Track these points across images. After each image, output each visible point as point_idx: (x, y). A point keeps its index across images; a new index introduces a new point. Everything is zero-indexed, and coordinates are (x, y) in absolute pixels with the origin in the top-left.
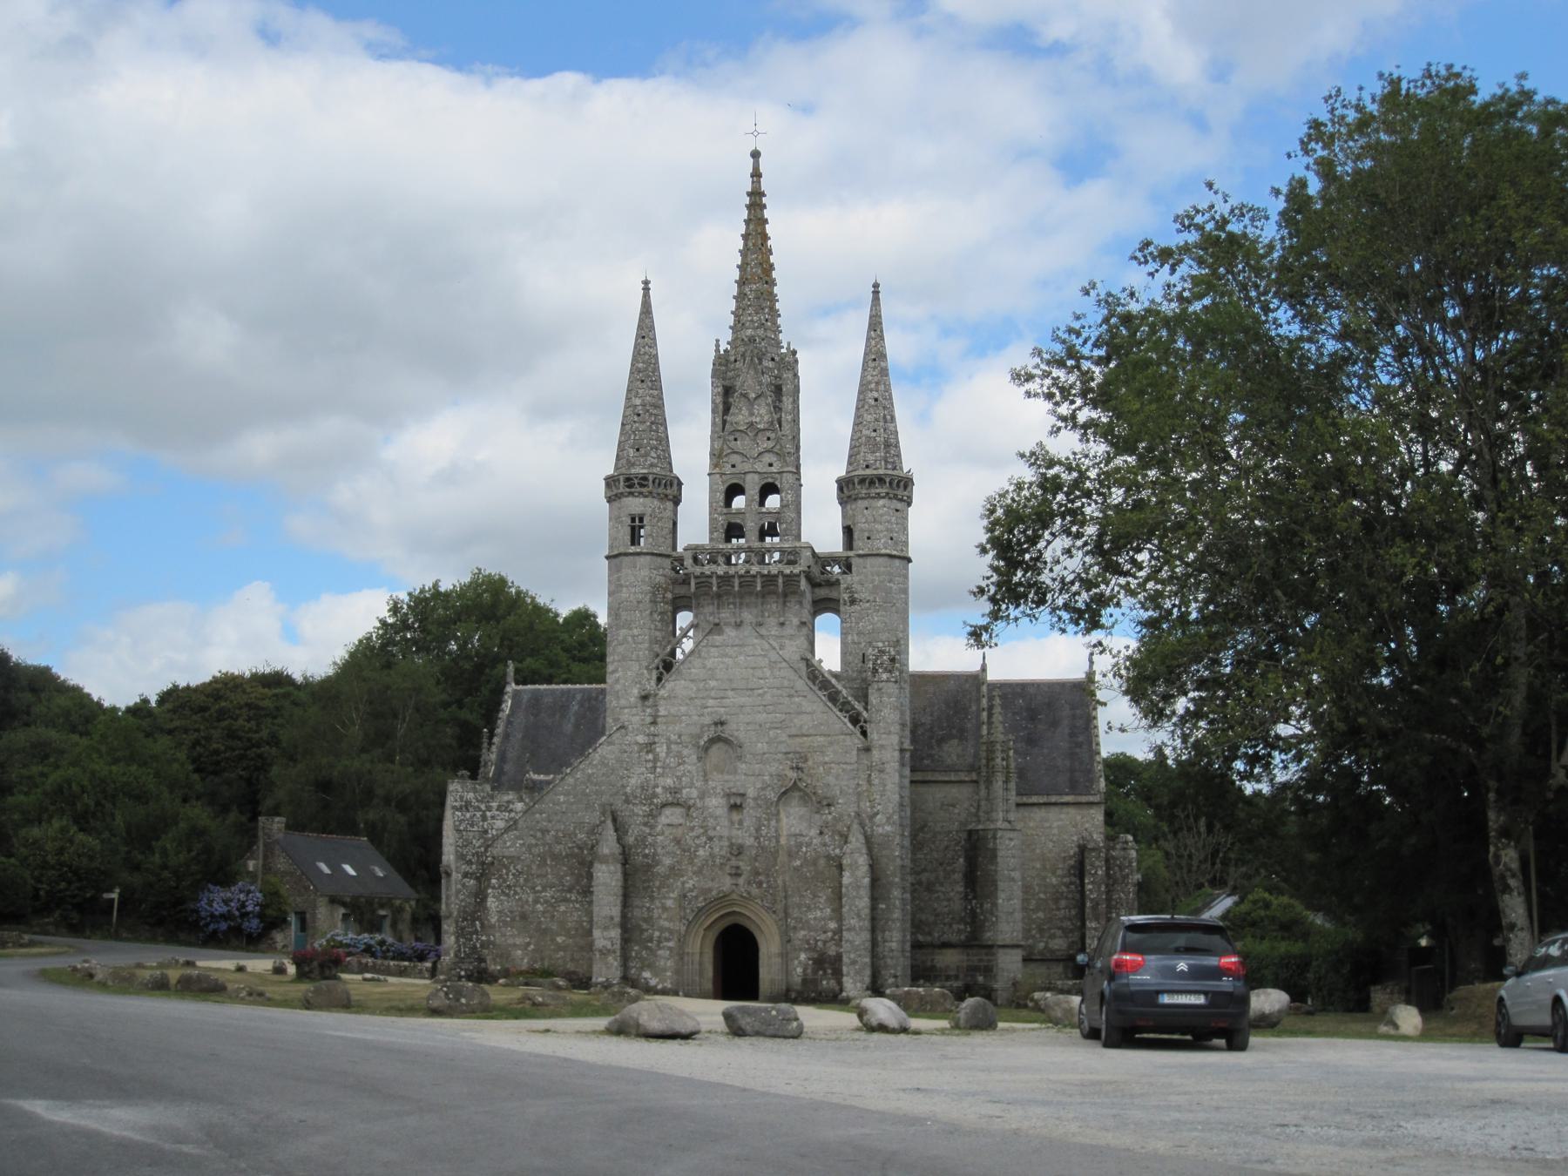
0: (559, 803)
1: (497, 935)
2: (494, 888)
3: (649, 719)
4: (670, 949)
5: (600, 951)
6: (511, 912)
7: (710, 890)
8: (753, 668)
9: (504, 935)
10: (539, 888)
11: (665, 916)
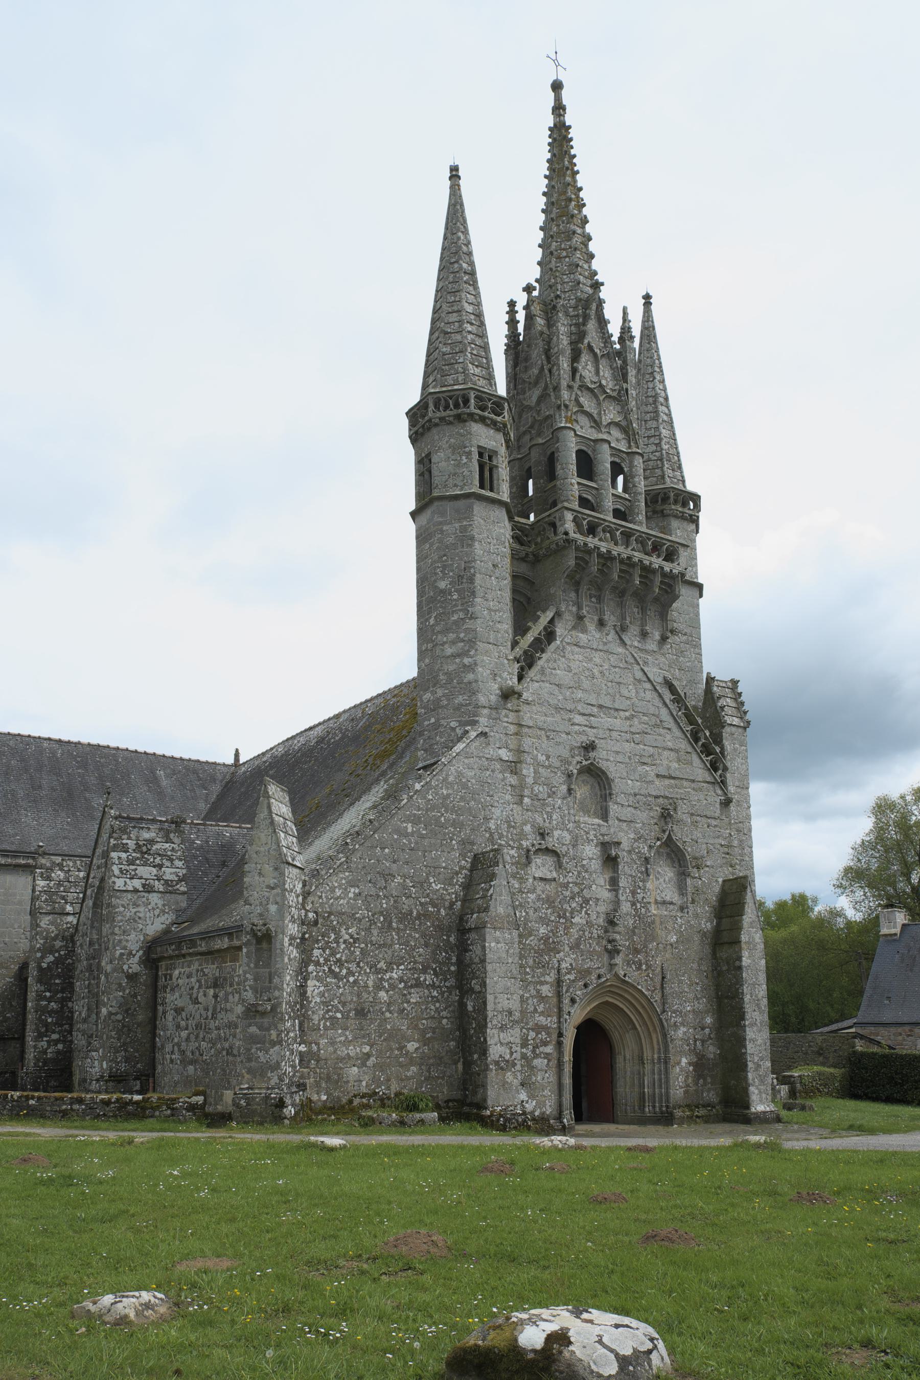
0: (406, 835)
1: (323, 1042)
2: (317, 963)
3: (512, 729)
4: (547, 1056)
5: (497, 1063)
6: (344, 1004)
7: (588, 972)
8: (619, 683)
9: (333, 1043)
10: (382, 965)
11: (541, 1008)
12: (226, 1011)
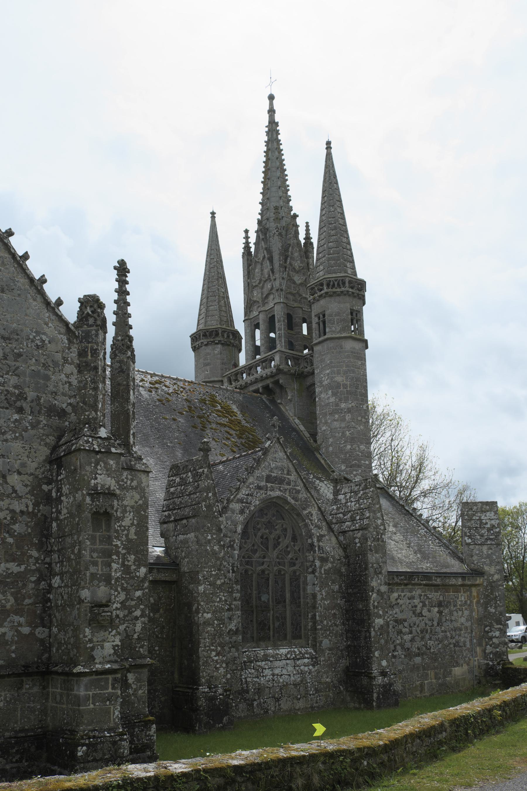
12: (452, 621)
